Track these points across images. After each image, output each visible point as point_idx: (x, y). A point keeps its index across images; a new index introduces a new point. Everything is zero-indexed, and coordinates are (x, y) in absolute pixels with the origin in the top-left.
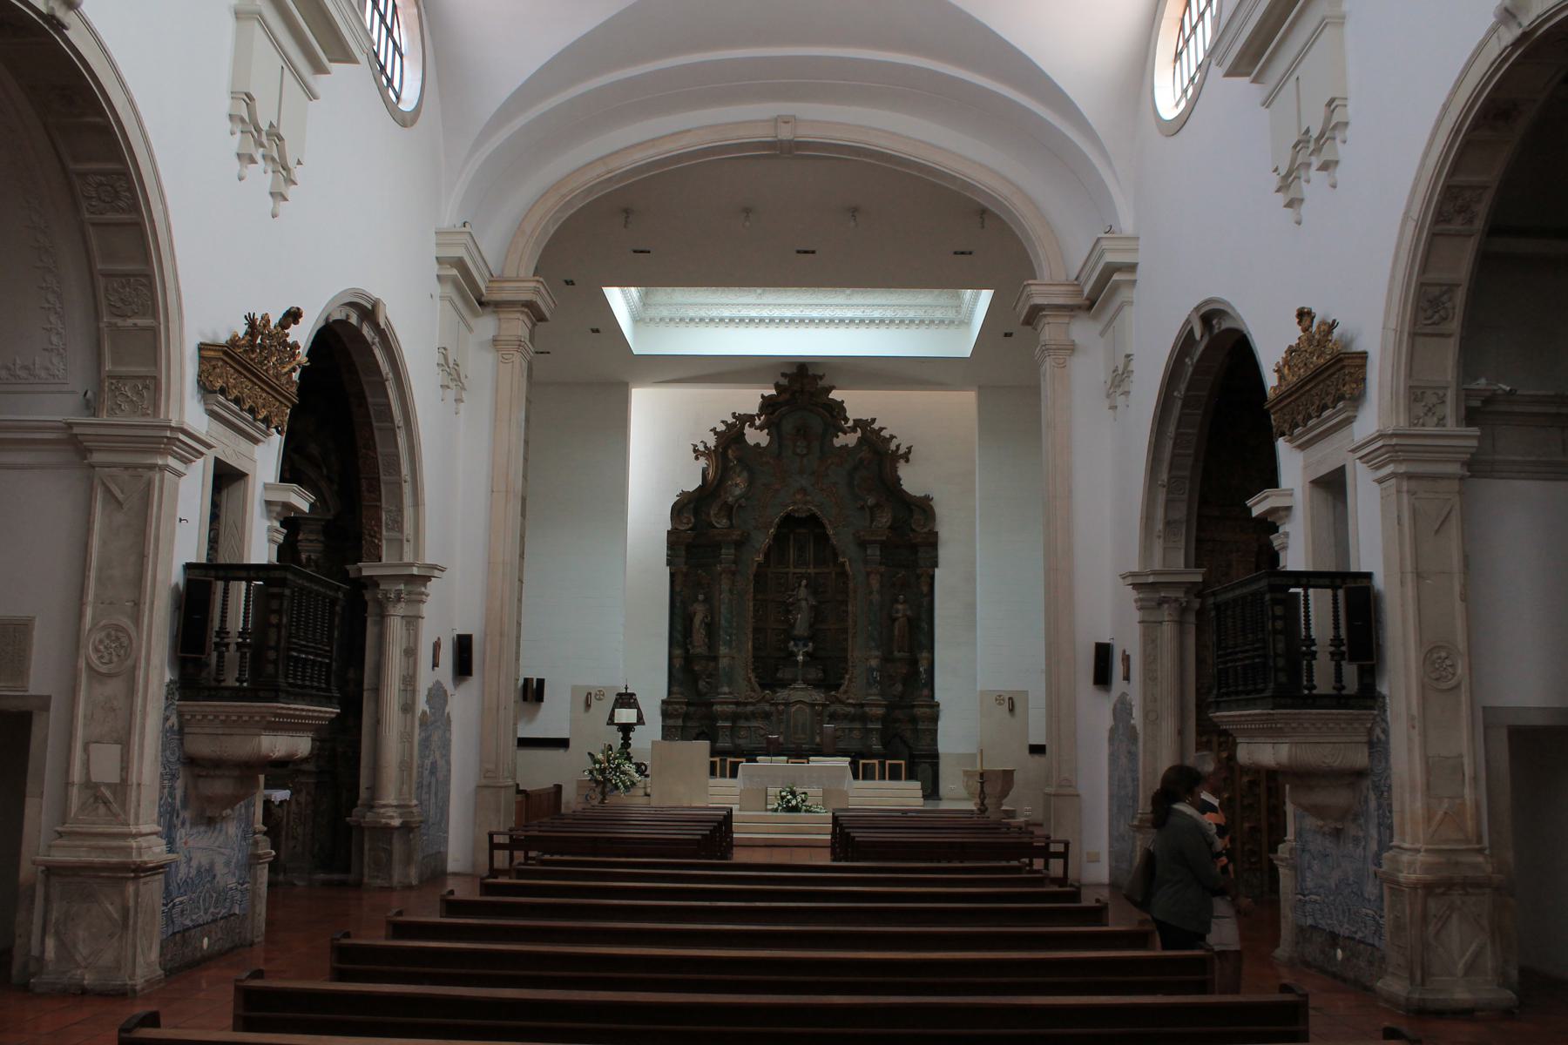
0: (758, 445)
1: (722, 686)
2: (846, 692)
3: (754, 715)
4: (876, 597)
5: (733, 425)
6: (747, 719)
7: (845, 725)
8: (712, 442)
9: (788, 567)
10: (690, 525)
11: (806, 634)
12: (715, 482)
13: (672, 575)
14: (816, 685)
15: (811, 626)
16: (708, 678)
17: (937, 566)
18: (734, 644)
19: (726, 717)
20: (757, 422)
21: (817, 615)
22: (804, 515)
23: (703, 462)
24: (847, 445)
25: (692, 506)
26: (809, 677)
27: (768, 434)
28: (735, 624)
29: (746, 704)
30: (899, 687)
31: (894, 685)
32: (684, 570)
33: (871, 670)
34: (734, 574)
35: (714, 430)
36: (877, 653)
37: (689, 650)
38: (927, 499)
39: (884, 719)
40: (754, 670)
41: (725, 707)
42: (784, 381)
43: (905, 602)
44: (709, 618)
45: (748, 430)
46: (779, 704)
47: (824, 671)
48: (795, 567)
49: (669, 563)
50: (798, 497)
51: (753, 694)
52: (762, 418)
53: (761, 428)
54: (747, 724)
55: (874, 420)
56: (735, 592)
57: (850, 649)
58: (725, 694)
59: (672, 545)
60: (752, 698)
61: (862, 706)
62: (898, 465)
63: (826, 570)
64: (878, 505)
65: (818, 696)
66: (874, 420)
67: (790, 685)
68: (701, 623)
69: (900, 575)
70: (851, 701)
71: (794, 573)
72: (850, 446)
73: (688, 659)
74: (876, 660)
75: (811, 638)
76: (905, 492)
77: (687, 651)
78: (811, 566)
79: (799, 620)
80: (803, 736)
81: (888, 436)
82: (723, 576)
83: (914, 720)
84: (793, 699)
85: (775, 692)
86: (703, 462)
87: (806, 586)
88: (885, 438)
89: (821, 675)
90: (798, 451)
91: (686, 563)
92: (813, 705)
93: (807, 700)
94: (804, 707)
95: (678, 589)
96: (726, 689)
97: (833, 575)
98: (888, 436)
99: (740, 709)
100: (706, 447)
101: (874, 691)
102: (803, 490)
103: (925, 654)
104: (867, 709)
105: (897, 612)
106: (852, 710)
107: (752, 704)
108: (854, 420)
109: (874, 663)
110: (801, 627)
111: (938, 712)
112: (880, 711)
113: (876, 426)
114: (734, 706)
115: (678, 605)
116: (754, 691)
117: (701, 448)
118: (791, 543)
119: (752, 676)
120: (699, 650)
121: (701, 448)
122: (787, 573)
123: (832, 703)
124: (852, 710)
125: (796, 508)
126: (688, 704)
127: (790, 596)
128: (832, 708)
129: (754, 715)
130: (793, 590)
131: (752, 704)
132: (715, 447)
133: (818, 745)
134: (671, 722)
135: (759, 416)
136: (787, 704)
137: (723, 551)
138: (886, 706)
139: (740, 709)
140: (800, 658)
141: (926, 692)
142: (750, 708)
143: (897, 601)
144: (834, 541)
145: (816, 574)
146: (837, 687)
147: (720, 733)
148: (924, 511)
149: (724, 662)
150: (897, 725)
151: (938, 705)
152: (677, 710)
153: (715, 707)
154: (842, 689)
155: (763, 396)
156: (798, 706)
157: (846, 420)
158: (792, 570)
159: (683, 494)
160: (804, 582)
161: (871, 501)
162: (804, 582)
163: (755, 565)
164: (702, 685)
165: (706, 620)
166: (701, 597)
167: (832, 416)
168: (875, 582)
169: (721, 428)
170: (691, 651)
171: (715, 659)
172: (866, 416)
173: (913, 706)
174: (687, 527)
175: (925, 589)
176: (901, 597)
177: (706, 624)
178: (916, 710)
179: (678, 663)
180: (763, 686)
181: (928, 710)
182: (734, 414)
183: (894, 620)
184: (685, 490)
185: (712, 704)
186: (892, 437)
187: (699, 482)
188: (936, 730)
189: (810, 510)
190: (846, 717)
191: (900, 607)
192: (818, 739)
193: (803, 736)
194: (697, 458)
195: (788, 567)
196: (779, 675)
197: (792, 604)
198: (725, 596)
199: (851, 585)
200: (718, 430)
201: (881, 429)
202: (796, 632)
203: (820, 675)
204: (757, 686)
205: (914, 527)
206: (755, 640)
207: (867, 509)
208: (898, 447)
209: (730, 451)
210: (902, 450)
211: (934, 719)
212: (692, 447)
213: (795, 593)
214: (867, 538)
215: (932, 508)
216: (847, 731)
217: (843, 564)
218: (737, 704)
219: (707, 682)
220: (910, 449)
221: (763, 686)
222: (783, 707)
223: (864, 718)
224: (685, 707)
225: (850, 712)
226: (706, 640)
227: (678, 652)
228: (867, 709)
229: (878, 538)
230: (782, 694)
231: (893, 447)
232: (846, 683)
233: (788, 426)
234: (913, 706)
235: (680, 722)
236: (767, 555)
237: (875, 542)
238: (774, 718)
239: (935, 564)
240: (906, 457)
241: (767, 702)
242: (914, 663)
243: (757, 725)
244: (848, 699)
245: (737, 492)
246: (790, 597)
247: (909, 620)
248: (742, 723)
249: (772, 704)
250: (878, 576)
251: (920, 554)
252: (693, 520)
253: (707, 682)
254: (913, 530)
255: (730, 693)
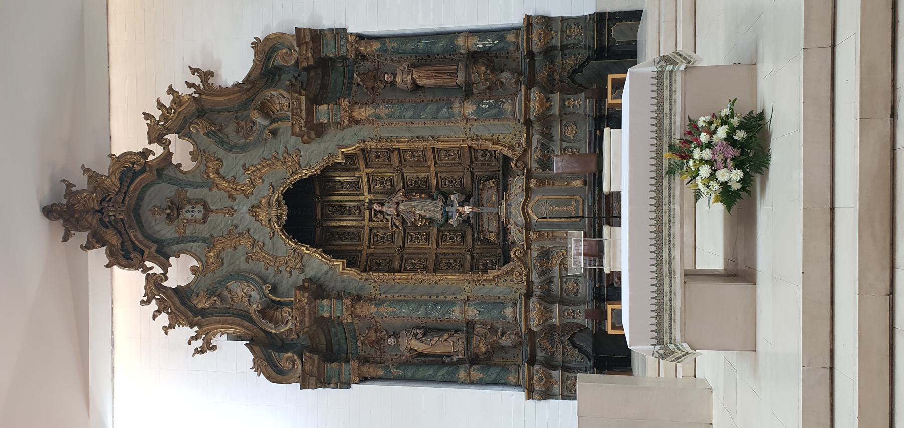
0: (194, 270)
1: (505, 318)
2: (511, 148)
3: (545, 272)
4: (383, 110)
5: (160, 302)
6: (550, 281)
7: (556, 147)
8: (184, 332)
9: (363, 227)
10: (296, 357)
11: (441, 203)
12: (246, 323)
13: (363, 380)
14: (504, 188)
15: (432, 198)
16: (497, 334)
17: (344, 30)
18: (451, 298)
19: (546, 313)
20: (157, 270)
21: (422, 189)
22: (285, 208)
23: (220, 340)
24: (191, 153)
25: (274, 354)
26: (494, 198)
27: (178, 257)
28: (424, 297)
29: (530, 283)
30: (506, 76)
31: (502, 83)
32: (356, 363)
33: (479, 112)
34: (357, 299)
35: (166, 329)
36: (456, 108)
37: (459, 359)
38: (256, 45)
39: (548, 88)
40: (485, 271)
41: (534, 314)
42: (82, 237)
43: (394, 75)
44: (418, 331)
45: (171, 283)
46: (527, 238)
47: (489, 178)
48: (363, 220)
49: (347, 385)
50: (262, 215)
51: (516, 273)
52: (148, 264)
53: (165, 266)
54: (557, 281)
55: (147, 116)
56: (383, 296)
57: (456, 145)
58: (515, 313)
59: (323, 382)
60: (520, 274)
61: (528, 123)
62: (216, 86)
63: (365, 180)
64: (264, 110)
65: (517, 184)
66: (147, 116)
67: (503, 222)
68: (422, 342)
69: (359, 80)
70: (523, 140)
71: (371, 219)
72: (192, 148)
73: (473, 360)
74: (466, 105)
75: (446, 196)
76: (249, 75)
77: (460, 362)
78: (361, 198)
79: (423, 213)
80: (573, 203)
81: (171, 97)
82: (358, 312)
83: (549, 52)
84: (521, 219)
85: (513, 243)
86: (220, 340)
87: (382, 205)
88: (173, 102)
89: (491, 183)
90: (199, 216)
91: (347, 361)
92: (528, 191)
93: (523, 200)
94: (530, 205)
95: (381, 373)
96: (509, 312)
97: (368, 171)
98: (171, 97)
99: (537, 290)
100: (195, 338)
101: (508, 107)
102: (253, 210)
103: (460, 41)
104: (533, 115)
105: (404, 82)
106: (536, 138)
107: (528, 276)
108: (150, 143)
109: (469, 109)
110: (432, 209)
111: (537, 17)
112: (535, 94)
113: (157, 113)
114: (532, 301)
115: (401, 372)
116: (512, 271)
117: (199, 343)
118: (334, 224)
119: (491, 274)
120: (459, 346)
121: (199, 343)
122: (371, 229)
123: (526, 165)
124: (536, 138)
125: (274, 219)
126: (532, 362)
127: (393, 223)
128: (534, 166)
129: (545, 272)
130: (388, 220)
131: (528, 276)
132: (192, 327)
133: (585, 183)
134: (557, 389)
135: (145, 270)
136: (528, 227)
137: (326, 315)
138: (529, 88)
139: (537, 290)
140: (467, 210)
141: (511, 37)
142: (535, 277)
143: (393, 84)
144: (316, 169)
145: (370, 193)
146: (507, 160)
147: (571, 320)
148: (273, 50)
149: (471, 313)
150: (557, 77)
151: (528, 18)
152: (541, 379)
153: (535, 329)
154: (508, 154)
155: (109, 266)
156: (530, 211)
157: (145, 153)
158: (366, 222)
159: (257, 367)
160: (377, 207)
161: (260, 121)
162: (377, 207)
163: (349, 271)
164: (506, 341)
165: (420, 336)
166: (392, 341)
167: (143, 171)
168: (361, 113)
169: (164, 319)
170: (461, 357)
171: (470, 325)
172: (143, 127)
173: (531, 54)
174: (298, 361)
175: (376, 46)
176: (386, 77)
177: (424, 335)
178: (535, 49)
179: (476, 374)
180: (507, 260)
181: (535, 31)
182: (143, 303)
183: (416, 87)
184: (251, 365)
185: (530, 330)
186: (171, 91)
187: (241, 346)
188: (563, 19)
189: (278, 201)
190: (544, 147)
191: (399, 80)
192: (577, 183)
193: (573, 203)
194: (214, 348)
195: (363, 227)
196: (492, 237)
197: (404, 221)
198: (385, 310)
199: (373, 145)
200: (167, 324)
201: (160, 105)
202: (439, 216)
203: (491, 185)
204: (508, 267)
205: (293, 62)
206: (449, 269)
207: (275, 125)
208: (190, 85)
209: (200, 306)
210: (197, 80)
211: (547, 21)
212: (197, 355)
213: (390, 218)
214: (303, 122)
215: (267, 39)
216: (565, 144)
217: (346, 156)
218: (528, 295)
219: (503, 334)
220: (194, 71)
221: (507, 260)
222: (532, 232)
223: (545, 119)
224: (537, 367)
225: (538, 140)
226: (446, 335)
227: (462, 374)
228: (533, 115)
229: (304, 108)
230: (516, 234)
231: (184, 91)
232: (500, 147)
233: (166, 231)
234: (531, 54)
235: (557, 374)
236: (337, 255)
237: (310, 112)
238: (549, 245)
239: (340, 33)
240: (206, 76)
241: (526, 253)
242: (473, 57)
243: (558, 268)
244: (520, 144)
245: (255, 295)
246: (396, 225)
247: (414, 66)
248: (556, 287)
249: (529, 247)
250: (357, 107)
251: (332, 55)
252: (290, 354)
253: (503, 334)
254: (297, 62)
255: (514, 304)
